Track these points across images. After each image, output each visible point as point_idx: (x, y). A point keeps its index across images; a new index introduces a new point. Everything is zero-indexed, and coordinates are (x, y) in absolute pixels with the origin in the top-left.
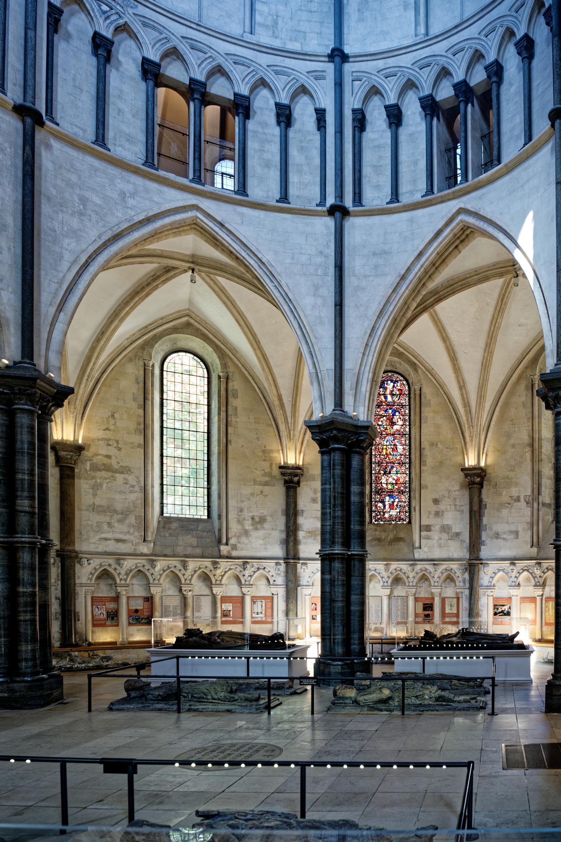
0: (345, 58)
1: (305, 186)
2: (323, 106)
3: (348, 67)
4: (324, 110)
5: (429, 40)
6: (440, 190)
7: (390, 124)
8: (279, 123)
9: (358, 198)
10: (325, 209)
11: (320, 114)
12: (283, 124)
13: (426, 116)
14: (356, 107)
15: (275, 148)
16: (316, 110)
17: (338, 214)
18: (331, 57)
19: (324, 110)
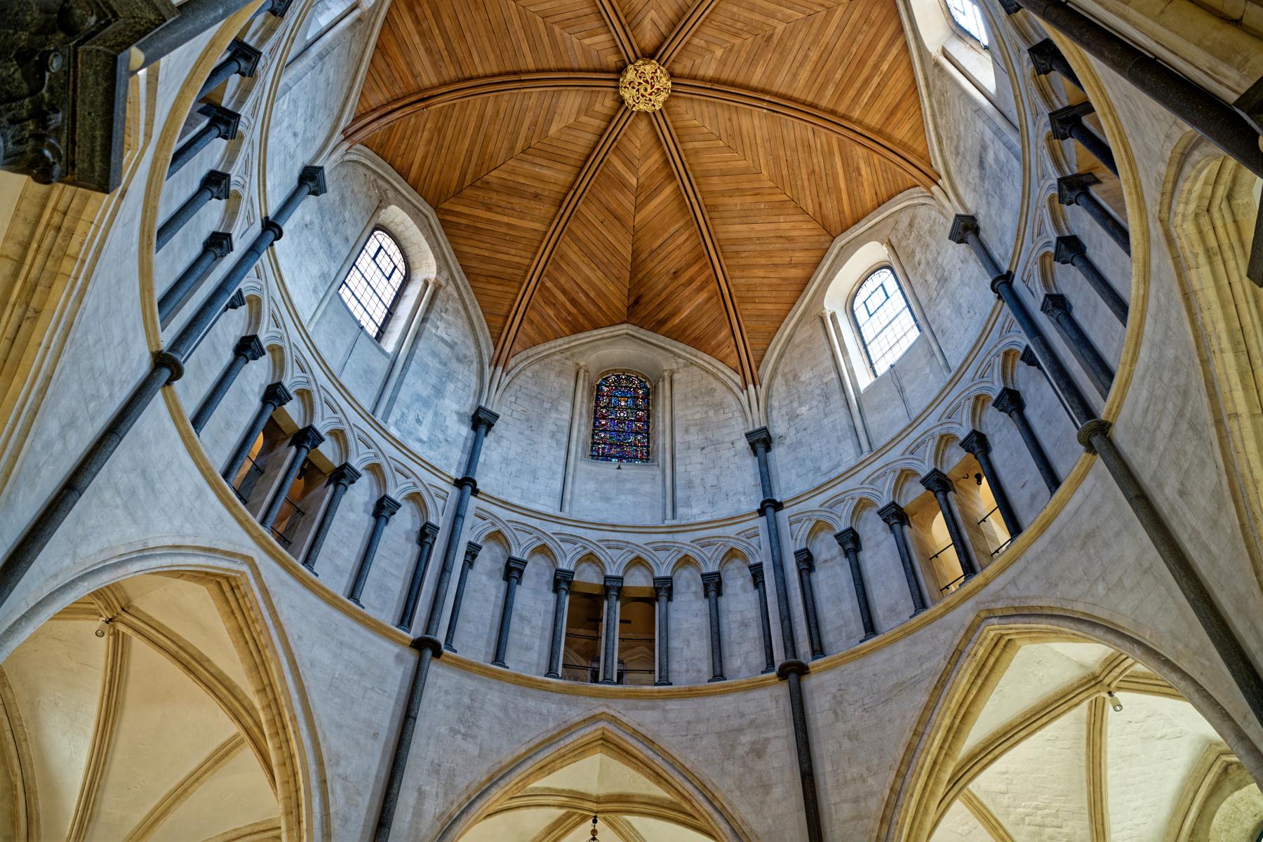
0: (778, 506)
1: (744, 654)
2: (758, 561)
3: (783, 515)
4: (761, 564)
5: (877, 453)
6: (934, 603)
7: (846, 553)
8: (706, 595)
9: (818, 650)
10: (774, 674)
11: (757, 573)
12: (712, 594)
13: (891, 528)
14: (798, 548)
15: (702, 622)
16: (751, 567)
17: (793, 677)
18: (762, 512)
19: (761, 564)
